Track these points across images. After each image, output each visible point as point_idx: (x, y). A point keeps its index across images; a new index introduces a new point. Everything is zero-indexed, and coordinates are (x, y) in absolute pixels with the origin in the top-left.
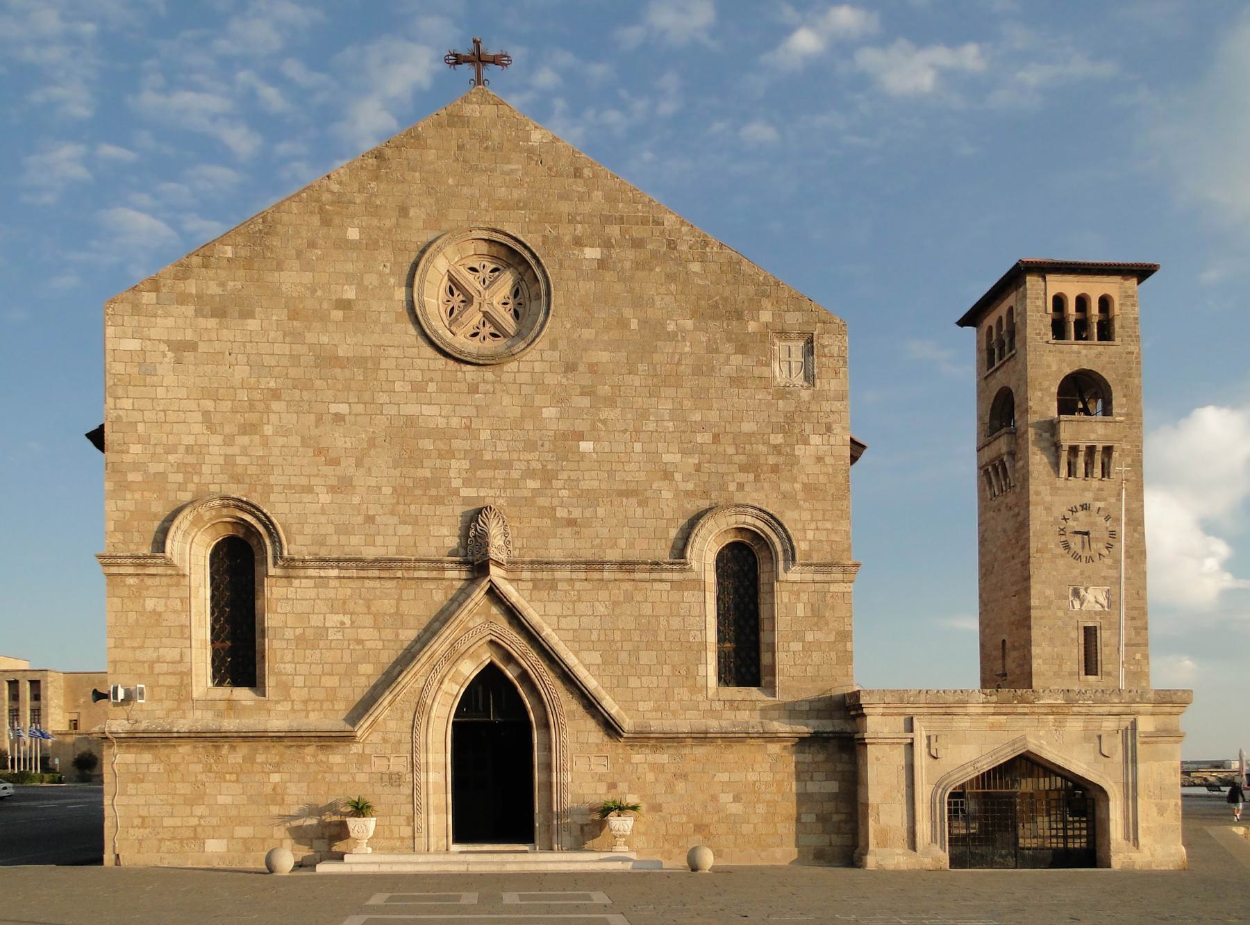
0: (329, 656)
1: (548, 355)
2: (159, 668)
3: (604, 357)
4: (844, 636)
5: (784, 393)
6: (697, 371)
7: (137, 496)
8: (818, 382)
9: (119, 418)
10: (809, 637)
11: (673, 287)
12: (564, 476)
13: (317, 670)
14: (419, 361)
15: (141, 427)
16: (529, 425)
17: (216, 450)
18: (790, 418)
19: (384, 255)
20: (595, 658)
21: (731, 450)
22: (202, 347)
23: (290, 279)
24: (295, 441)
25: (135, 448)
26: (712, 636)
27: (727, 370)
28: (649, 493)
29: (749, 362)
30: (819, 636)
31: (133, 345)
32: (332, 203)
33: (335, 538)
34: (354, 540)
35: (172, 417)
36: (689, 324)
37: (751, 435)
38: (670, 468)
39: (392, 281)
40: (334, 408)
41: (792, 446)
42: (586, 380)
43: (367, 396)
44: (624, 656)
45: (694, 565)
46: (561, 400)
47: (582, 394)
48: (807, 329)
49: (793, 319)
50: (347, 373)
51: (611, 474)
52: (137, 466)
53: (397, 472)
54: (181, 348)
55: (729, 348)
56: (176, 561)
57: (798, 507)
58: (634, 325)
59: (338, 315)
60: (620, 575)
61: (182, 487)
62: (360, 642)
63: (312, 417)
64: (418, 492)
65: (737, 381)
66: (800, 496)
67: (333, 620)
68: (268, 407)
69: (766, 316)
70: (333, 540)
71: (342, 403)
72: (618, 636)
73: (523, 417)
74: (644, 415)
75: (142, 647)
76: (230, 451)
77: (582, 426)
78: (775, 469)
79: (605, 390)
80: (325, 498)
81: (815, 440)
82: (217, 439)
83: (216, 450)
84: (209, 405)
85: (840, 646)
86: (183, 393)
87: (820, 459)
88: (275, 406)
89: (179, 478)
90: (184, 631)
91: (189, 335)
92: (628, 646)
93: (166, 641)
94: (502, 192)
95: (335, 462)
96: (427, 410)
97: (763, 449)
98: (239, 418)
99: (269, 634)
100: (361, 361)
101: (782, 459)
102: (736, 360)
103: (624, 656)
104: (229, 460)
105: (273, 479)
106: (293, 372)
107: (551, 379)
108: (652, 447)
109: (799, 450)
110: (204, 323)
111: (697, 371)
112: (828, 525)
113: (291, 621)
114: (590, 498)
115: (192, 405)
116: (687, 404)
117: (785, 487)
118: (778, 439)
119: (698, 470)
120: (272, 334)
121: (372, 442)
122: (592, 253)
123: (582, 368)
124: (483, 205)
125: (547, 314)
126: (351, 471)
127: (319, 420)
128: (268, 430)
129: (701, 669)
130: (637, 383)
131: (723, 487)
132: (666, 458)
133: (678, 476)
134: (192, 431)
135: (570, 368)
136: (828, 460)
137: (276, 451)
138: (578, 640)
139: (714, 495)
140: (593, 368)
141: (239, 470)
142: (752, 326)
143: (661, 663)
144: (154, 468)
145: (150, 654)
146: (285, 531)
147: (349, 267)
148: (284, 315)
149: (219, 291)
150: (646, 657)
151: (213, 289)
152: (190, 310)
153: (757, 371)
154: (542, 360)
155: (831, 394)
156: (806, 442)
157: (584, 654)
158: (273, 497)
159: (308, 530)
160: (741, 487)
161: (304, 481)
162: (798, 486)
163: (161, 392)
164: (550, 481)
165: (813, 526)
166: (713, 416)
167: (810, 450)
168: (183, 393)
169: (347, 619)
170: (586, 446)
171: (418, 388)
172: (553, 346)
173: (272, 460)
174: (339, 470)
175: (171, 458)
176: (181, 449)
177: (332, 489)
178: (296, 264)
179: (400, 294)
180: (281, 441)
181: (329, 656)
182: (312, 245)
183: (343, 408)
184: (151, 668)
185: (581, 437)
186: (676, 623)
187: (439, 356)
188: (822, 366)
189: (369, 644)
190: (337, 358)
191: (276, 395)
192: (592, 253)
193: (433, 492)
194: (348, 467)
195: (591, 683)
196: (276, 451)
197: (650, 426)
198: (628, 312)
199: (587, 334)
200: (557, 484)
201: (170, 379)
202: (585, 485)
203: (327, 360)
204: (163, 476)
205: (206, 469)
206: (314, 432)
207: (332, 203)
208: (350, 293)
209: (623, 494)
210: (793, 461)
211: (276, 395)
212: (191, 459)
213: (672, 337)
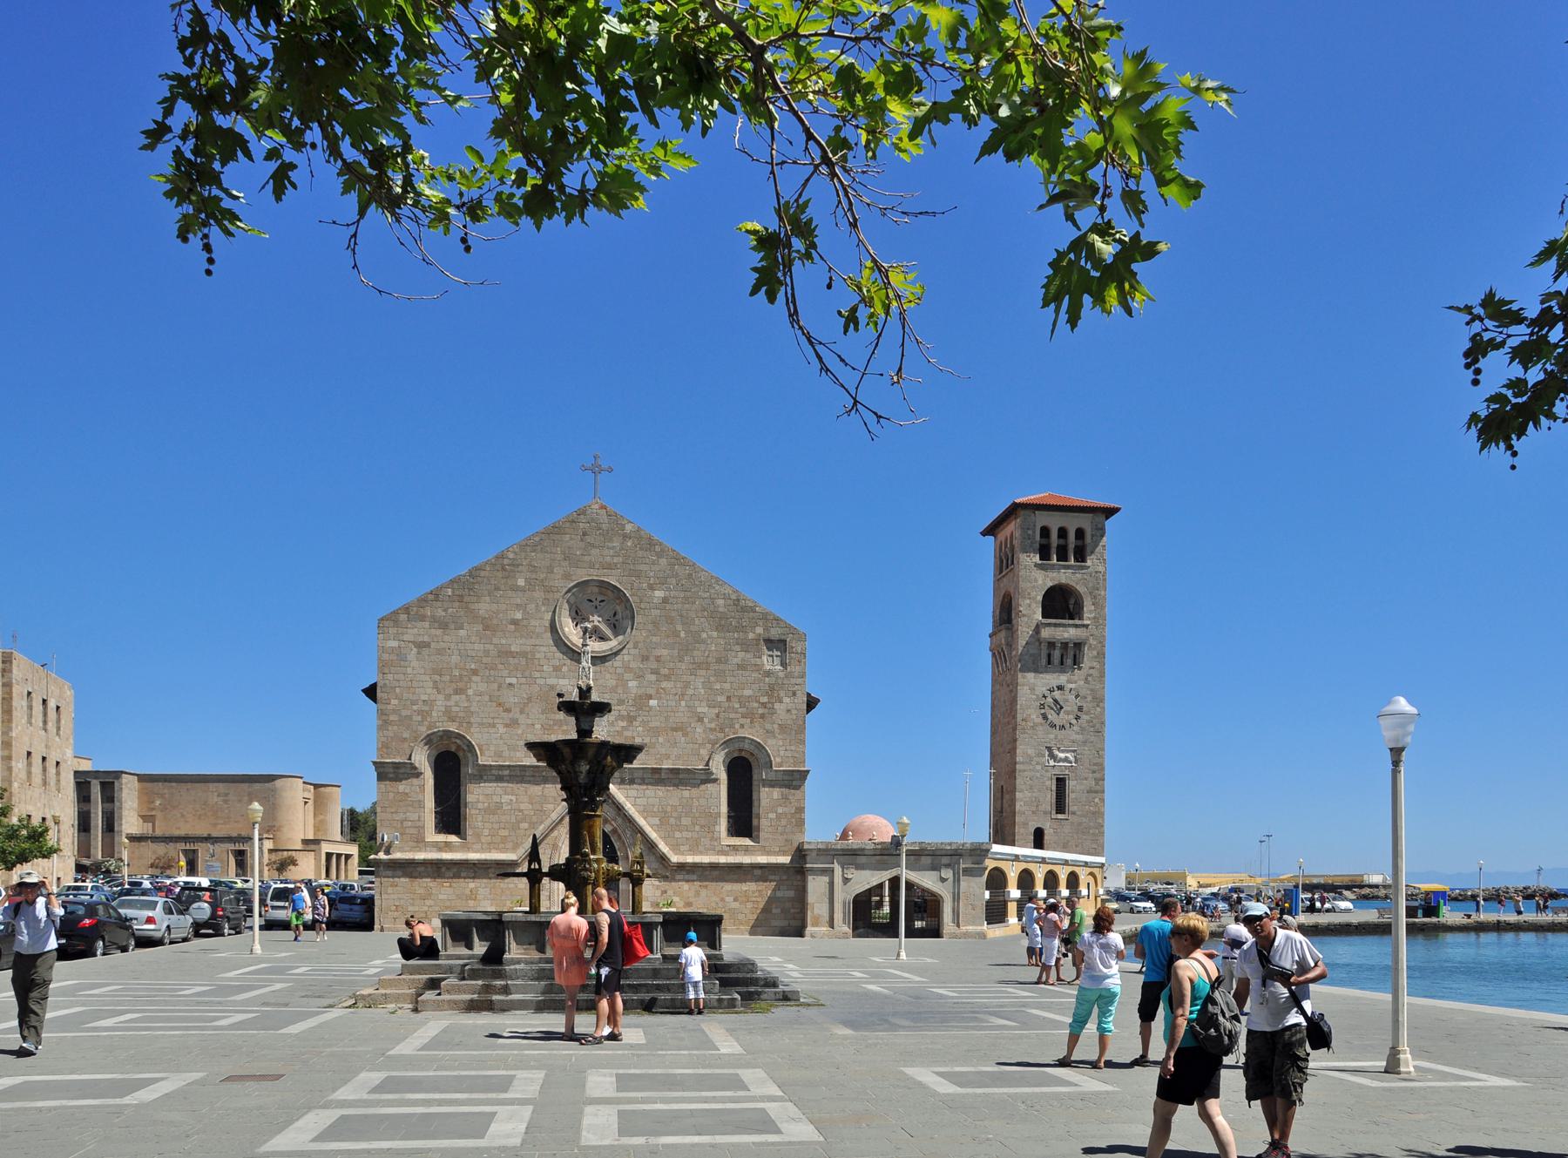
0: (503, 818)
1: (633, 651)
2: (405, 824)
3: (665, 652)
4: (801, 810)
5: (768, 674)
6: (719, 661)
7: (395, 728)
8: (789, 668)
9: (385, 684)
10: (780, 810)
11: (706, 613)
12: (639, 719)
13: (496, 826)
15: (398, 690)
16: (620, 690)
17: (440, 702)
18: (772, 688)
19: (539, 594)
20: (656, 821)
21: (737, 706)
22: (433, 645)
23: (484, 607)
24: (487, 698)
25: (394, 702)
26: (724, 809)
27: (735, 661)
28: (689, 729)
29: (749, 656)
30: (786, 810)
31: (394, 644)
33: (507, 752)
34: (518, 754)
35: (415, 684)
36: (715, 634)
37: (749, 697)
38: (701, 715)
40: (508, 680)
41: (773, 703)
42: (654, 665)
43: (527, 674)
44: (672, 821)
45: (714, 771)
46: (639, 677)
47: (652, 673)
48: (783, 637)
49: (775, 633)
50: (516, 661)
51: (667, 718)
52: (395, 711)
53: (544, 717)
54: (421, 646)
55: (738, 648)
56: (417, 765)
57: (775, 737)
58: (683, 634)
60: (671, 776)
61: (420, 723)
62: (521, 811)
63: (495, 686)
64: (556, 728)
65: (741, 667)
66: (777, 731)
67: (506, 798)
68: (470, 679)
69: (759, 630)
70: (506, 754)
72: (669, 809)
73: (617, 686)
74: (687, 685)
75: (396, 812)
76: (448, 704)
77: (652, 691)
78: (762, 716)
79: (666, 671)
80: (502, 730)
81: (787, 700)
82: (441, 697)
83: (440, 702)
84: (437, 678)
85: (798, 816)
86: (422, 671)
87: (788, 711)
88: (475, 678)
89: (419, 718)
90: (421, 804)
91: (426, 639)
92: (675, 814)
93: (410, 808)
94: (608, 559)
95: (508, 710)
96: (562, 682)
97: (756, 705)
98: (454, 685)
99: (469, 806)
100: (524, 654)
101: (766, 711)
102: (741, 655)
103: (672, 821)
104: (447, 711)
105: (472, 720)
106: (485, 660)
107: (633, 665)
108: (691, 703)
109: (777, 706)
110: (433, 631)
111: (719, 661)
112: (793, 748)
113: (481, 798)
114: (656, 732)
115: (427, 678)
116: (712, 679)
117: (768, 726)
118: (765, 699)
119: (718, 717)
120: (473, 639)
121: (530, 699)
122: (659, 594)
123: (652, 659)
124: (597, 566)
125: (632, 629)
126: (517, 715)
127: (500, 686)
128: (470, 692)
129: (717, 828)
130: (683, 668)
131: (732, 726)
132: (699, 710)
133: (706, 720)
134: (426, 692)
135: (645, 658)
136: (794, 712)
137: (474, 704)
138: (645, 812)
139: (727, 730)
140: (658, 659)
141: (454, 714)
142: (751, 636)
143: (694, 824)
144: (404, 713)
145: (401, 816)
146: (480, 750)
147: (519, 601)
148: (480, 627)
149: (444, 614)
150: (685, 821)
151: (440, 613)
152: (427, 624)
153: (753, 661)
155: (796, 674)
156: (781, 702)
157: (649, 819)
158: (472, 730)
159: (492, 748)
160: (742, 726)
161: (491, 721)
162: (776, 726)
163: (409, 670)
164: (632, 722)
165: (784, 748)
166: (727, 686)
167: (783, 706)
168: (422, 671)
169: (513, 798)
170: (653, 703)
171: (557, 669)
172: (635, 648)
173: (472, 709)
174: (511, 715)
175: (415, 707)
176: (420, 703)
177: (507, 726)
178: (488, 599)
179: (548, 616)
180: (478, 698)
181: (503, 818)
182: (497, 589)
183: (514, 681)
184: (402, 823)
185: (650, 697)
186: (703, 802)
188: (791, 658)
189: (526, 812)
191: (475, 672)
192: (659, 594)
193: (565, 728)
194: (515, 714)
195: (653, 835)
196: (474, 704)
197: (690, 692)
198: (679, 627)
199: (654, 639)
200: (637, 724)
201: (415, 663)
202: (652, 724)
203: (506, 654)
204: (410, 718)
205: (434, 714)
206: (497, 693)
208: (519, 616)
209: (675, 729)
210: (773, 712)
211: (475, 672)
212: (426, 708)
213: (703, 642)
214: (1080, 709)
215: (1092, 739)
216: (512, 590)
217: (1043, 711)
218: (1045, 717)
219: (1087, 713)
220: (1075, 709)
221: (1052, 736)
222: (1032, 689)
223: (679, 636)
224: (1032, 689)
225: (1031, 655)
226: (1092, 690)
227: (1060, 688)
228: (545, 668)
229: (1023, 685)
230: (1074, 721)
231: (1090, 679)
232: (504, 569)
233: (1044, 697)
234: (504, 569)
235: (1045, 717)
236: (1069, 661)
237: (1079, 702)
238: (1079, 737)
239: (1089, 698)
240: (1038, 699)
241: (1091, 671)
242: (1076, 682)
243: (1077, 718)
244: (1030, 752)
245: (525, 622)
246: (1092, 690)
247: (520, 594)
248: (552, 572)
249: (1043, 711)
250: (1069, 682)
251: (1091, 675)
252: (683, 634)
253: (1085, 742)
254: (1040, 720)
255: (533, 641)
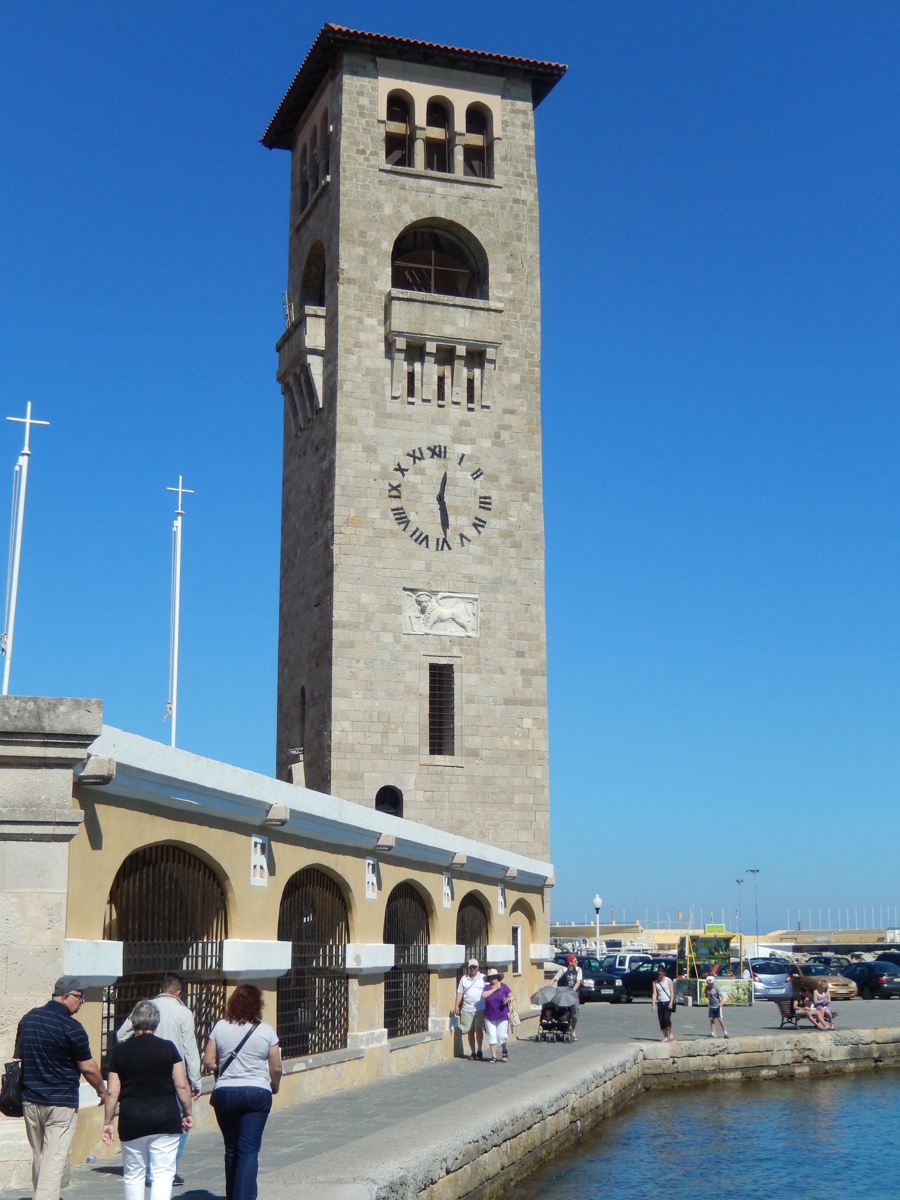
214: (485, 503)
215: (514, 573)
217: (396, 503)
218: (401, 517)
219: (503, 514)
220: (474, 503)
221: (418, 565)
222: (370, 450)
224: (370, 450)
225: (368, 372)
226: (512, 462)
227: (437, 452)
229: (350, 440)
230: (471, 532)
231: (505, 435)
233: (400, 469)
235: (401, 517)
236: (457, 392)
237: (480, 487)
238: (484, 571)
239: (506, 480)
240: (383, 475)
241: (508, 419)
242: (473, 441)
243: (479, 524)
244: (365, 598)
246: (512, 462)
249: (396, 503)
250: (457, 440)
251: (508, 428)
253: (496, 584)
254: (390, 523)
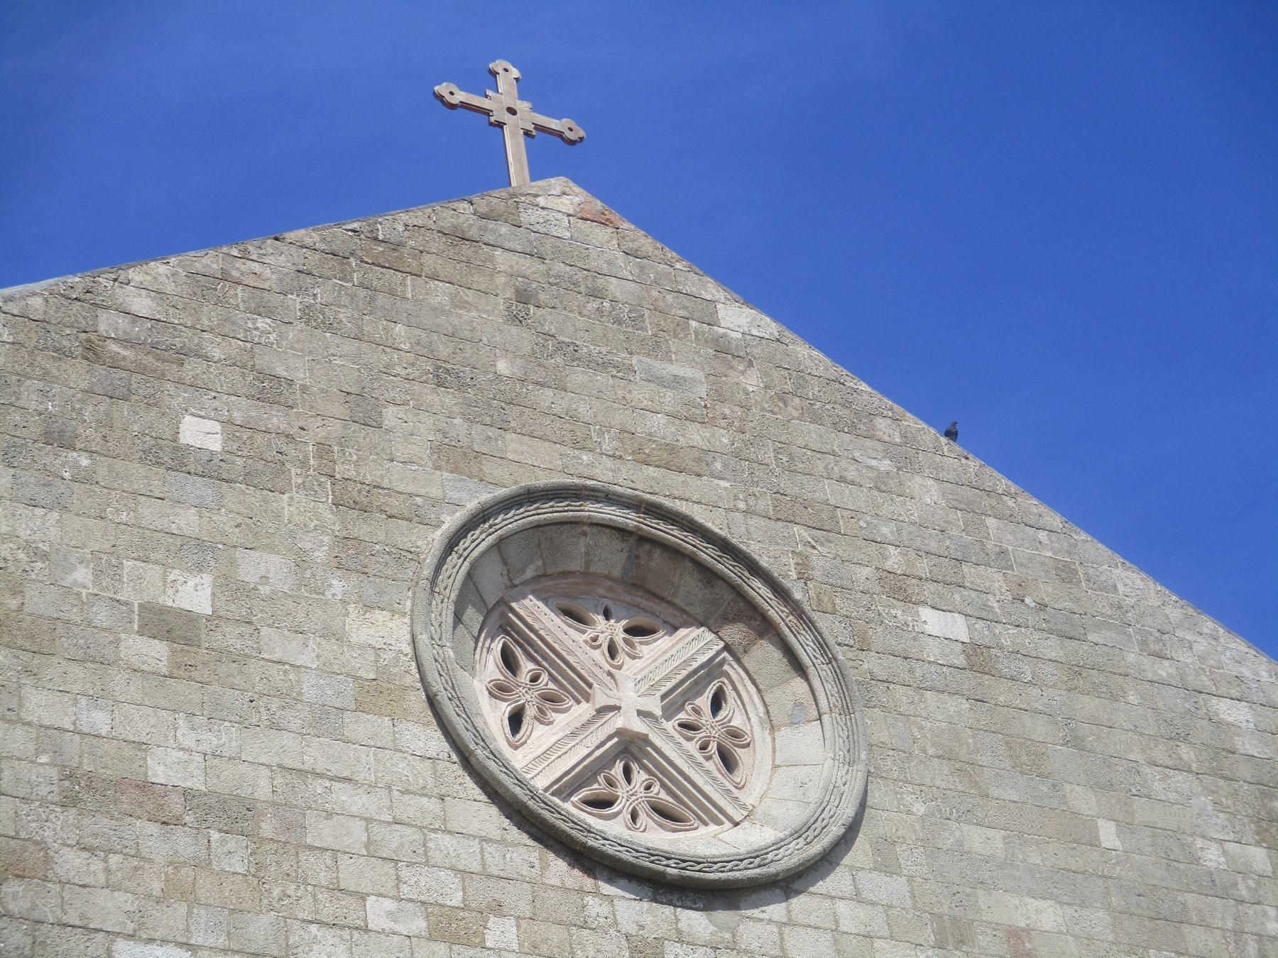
11: (1186, 752)
14: (446, 841)
32: (126, 342)
39: (338, 586)
50: (183, 843)
58: (1108, 834)
59: (157, 652)
71: (164, 941)
147: (187, 521)
154: (858, 897)
172: (887, 866)
187: (515, 834)
190: (145, 787)
198: (1082, 799)
207: (126, 342)
216: (151, 456)
223: (1094, 843)
228: (378, 911)
232: (92, 352)
234: (92, 352)
245: (231, 637)
247: (199, 489)
248: (371, 422)
252: (1108, 834)
255: (287, 748)
